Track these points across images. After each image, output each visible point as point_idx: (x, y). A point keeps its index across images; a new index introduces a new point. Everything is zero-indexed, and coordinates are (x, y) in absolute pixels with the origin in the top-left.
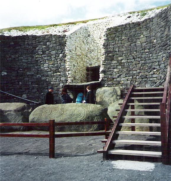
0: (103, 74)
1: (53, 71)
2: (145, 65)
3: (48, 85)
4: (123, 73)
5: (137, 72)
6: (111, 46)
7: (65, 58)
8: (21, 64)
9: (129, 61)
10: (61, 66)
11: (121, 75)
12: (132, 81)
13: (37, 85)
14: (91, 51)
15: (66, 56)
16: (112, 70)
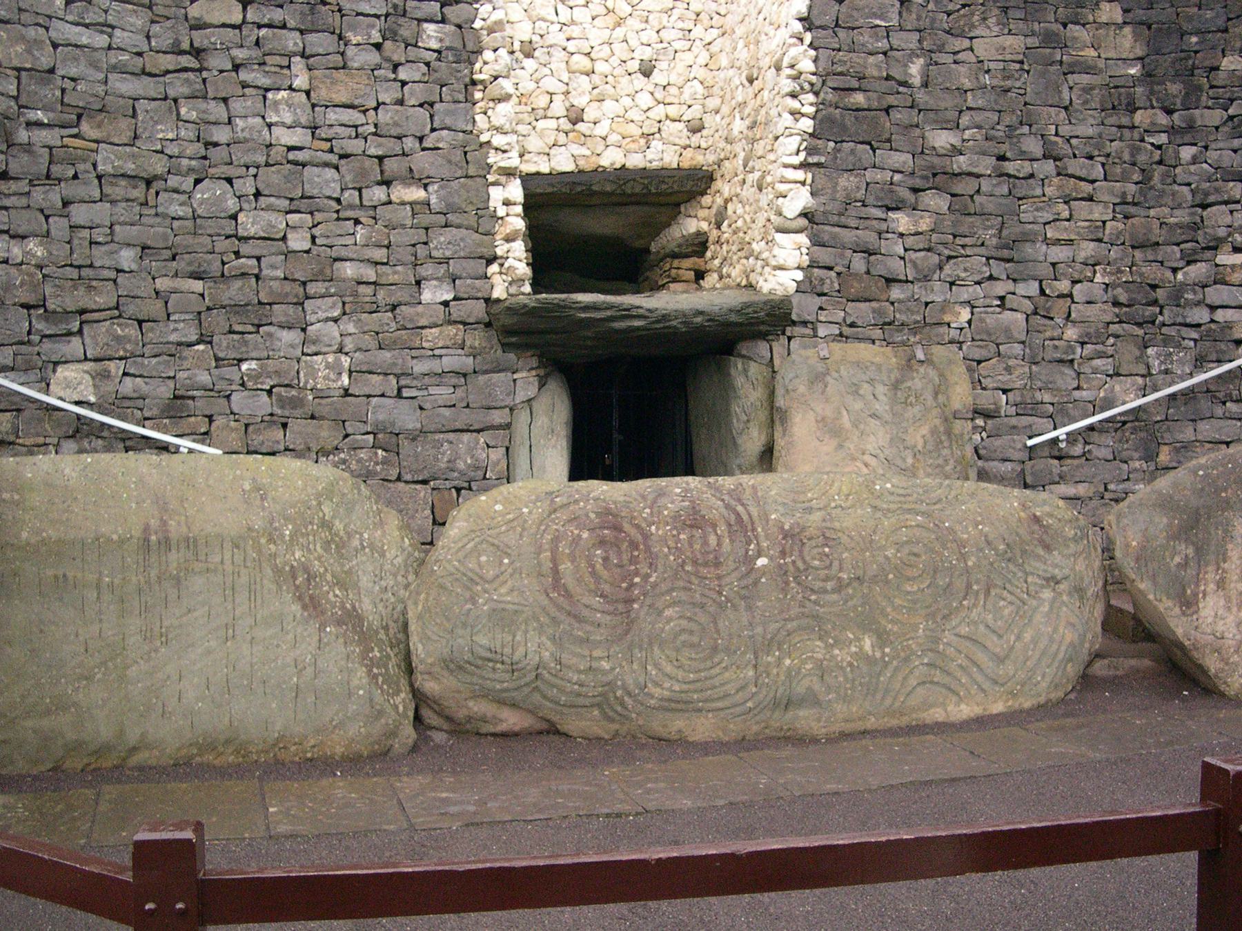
0: (803, 239)
1: (353, 163)
2: (1143, 212)
3: (304, 284)
4: (963, 246)
5: (1082, 256)
6: (865, 38)
7: (477, 66)
8: (45, 62)
9: (1010, 167)
10: (433, 130)
11: (949, 258)
12: (1035, 313)
13: (198, 286)
14: (519, 55)
15: (479, 52)
16: (879, 213)
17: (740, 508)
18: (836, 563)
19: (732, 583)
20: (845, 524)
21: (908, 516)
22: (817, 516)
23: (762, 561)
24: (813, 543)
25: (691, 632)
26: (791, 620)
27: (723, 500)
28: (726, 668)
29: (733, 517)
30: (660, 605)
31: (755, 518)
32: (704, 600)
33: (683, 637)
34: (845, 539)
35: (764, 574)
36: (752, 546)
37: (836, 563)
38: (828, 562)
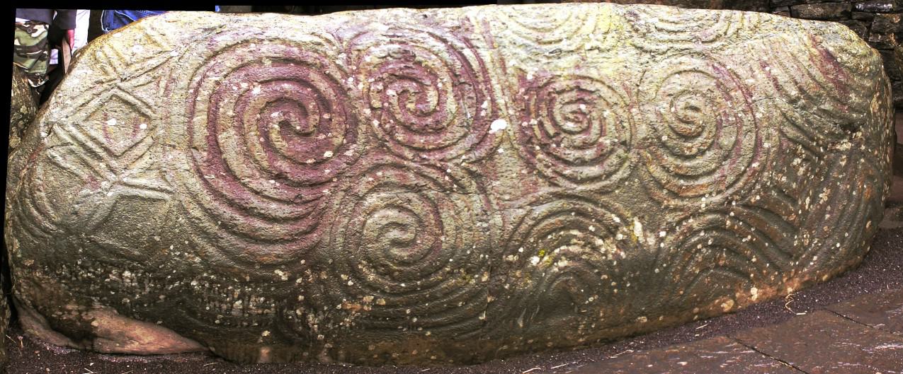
17: (467, 52)
18: (596, 125)
19: (458, 155)
20: (604, 72)
21: (683, 59)
22: (567, 63)
23: (498, 126)
24: (567, 97)
25: (403, 227)
26: (537, 202)
27: (445, 41)
28: (451, 273)
29: (458, 64)
30: (361, 188)
31: (489, 66)
32: (422, 182)
33: (395, 234)
34: (605, 92)
35: (501, 142)
36: (485, 105)
37: (596, 125)
38: (585, 125)
